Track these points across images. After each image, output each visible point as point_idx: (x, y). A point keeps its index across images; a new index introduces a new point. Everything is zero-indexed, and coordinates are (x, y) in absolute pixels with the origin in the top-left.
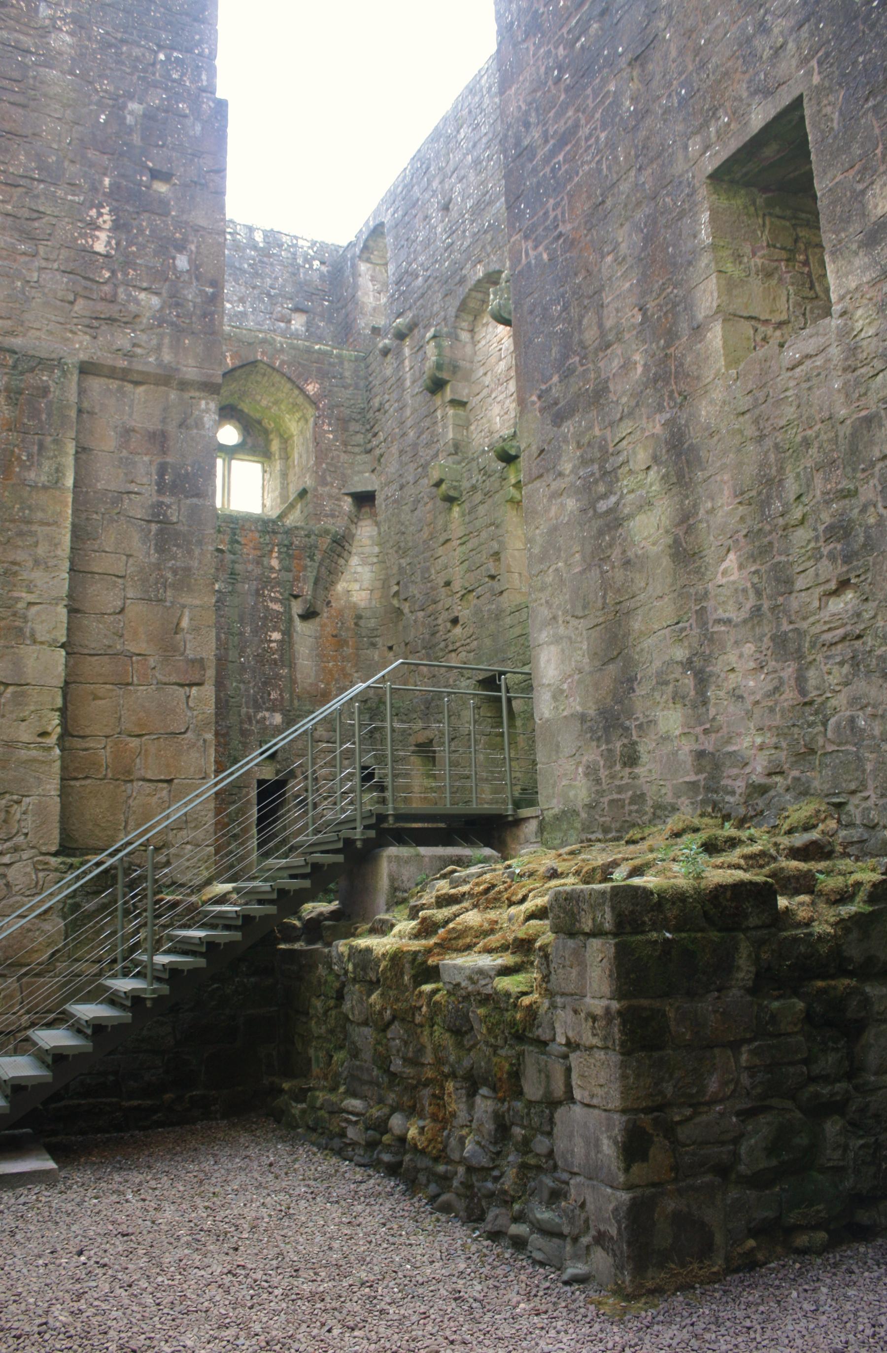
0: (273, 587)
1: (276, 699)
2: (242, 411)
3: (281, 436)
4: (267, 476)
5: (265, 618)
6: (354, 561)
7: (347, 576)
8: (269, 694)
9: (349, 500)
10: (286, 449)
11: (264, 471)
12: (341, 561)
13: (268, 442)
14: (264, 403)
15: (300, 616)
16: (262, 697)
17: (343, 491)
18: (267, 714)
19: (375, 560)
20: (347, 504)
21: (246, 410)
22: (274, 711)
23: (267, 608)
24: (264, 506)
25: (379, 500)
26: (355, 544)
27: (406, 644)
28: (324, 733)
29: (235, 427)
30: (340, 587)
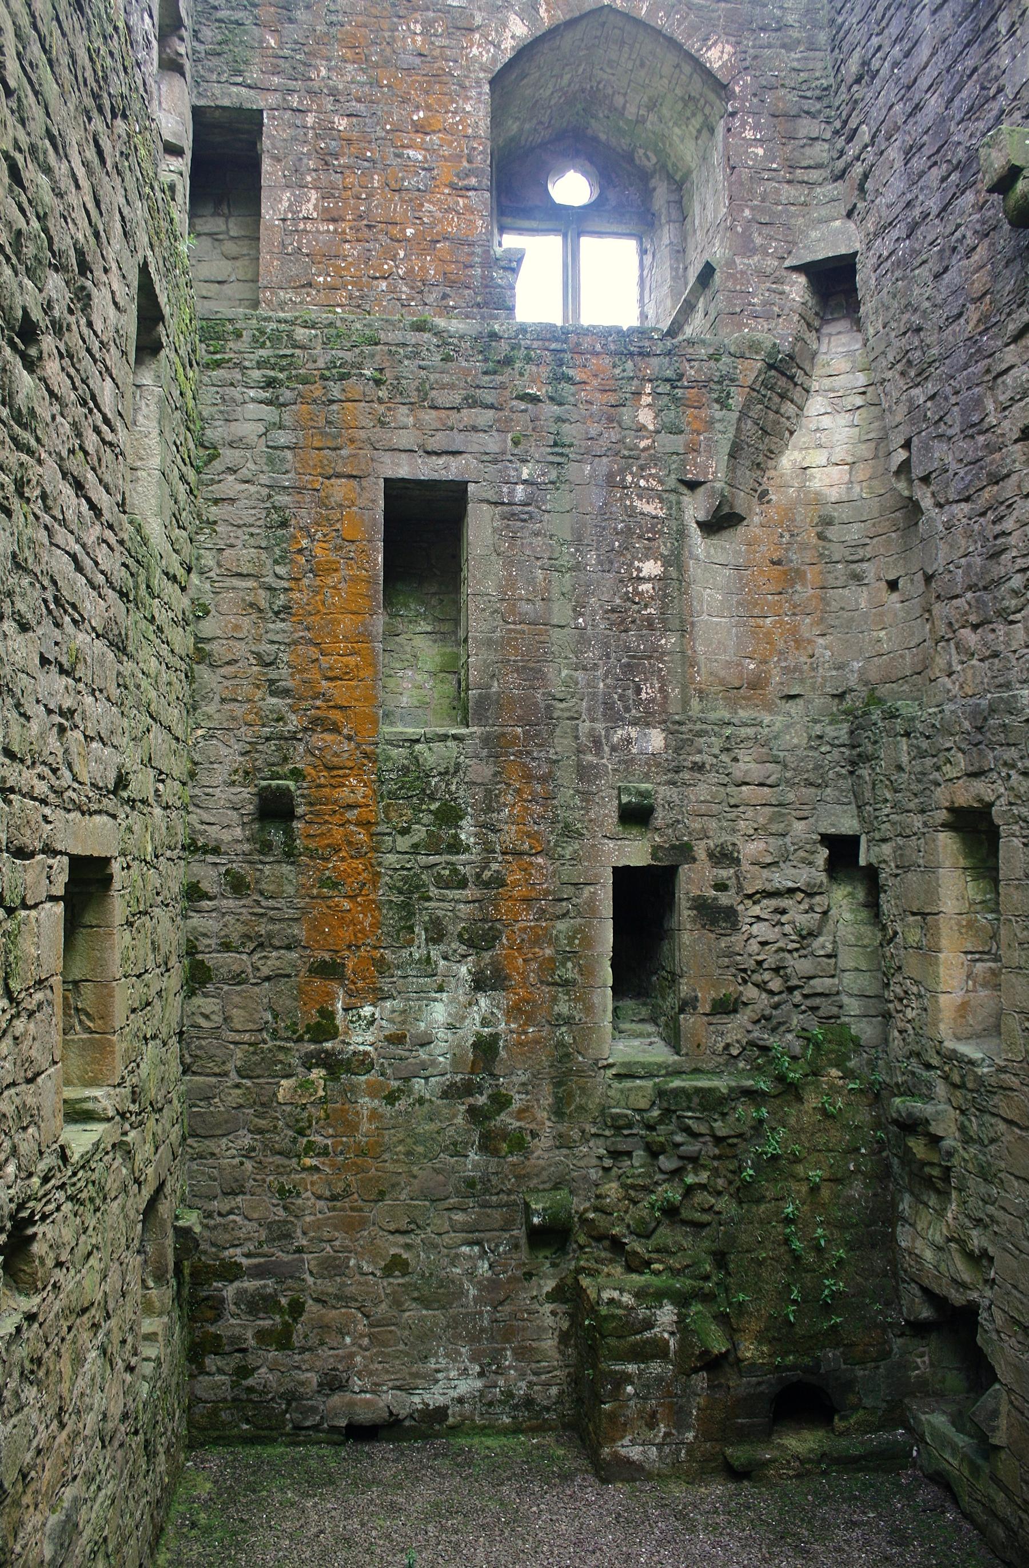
0: (642, 468)
1: (653, 700)
2: (595, 139)
3: (670, 177)
4: (648, 259)
5: (629, 531)
6: (816, 405)
7: (801, 438)
8: (638, 691)
9: (802, 280)
10: (680, 202)
11: (643, 252)
12: (789, 408)
13: (648, 193)
14: (631, 112)
15: (700, 524)
16: (621, 697)
17: (787, 263)
18: (633, 732)
19: (859, 401)
20: (797, 288)
21: (603, 137)
22: (648, 725)
23: (631, 512)
24: (643, 316)
25: (865, 277)
26: (818, 371)
27: (928, 579)
28: (753, 766)
29: (585, 174)
30: (788, 460)
